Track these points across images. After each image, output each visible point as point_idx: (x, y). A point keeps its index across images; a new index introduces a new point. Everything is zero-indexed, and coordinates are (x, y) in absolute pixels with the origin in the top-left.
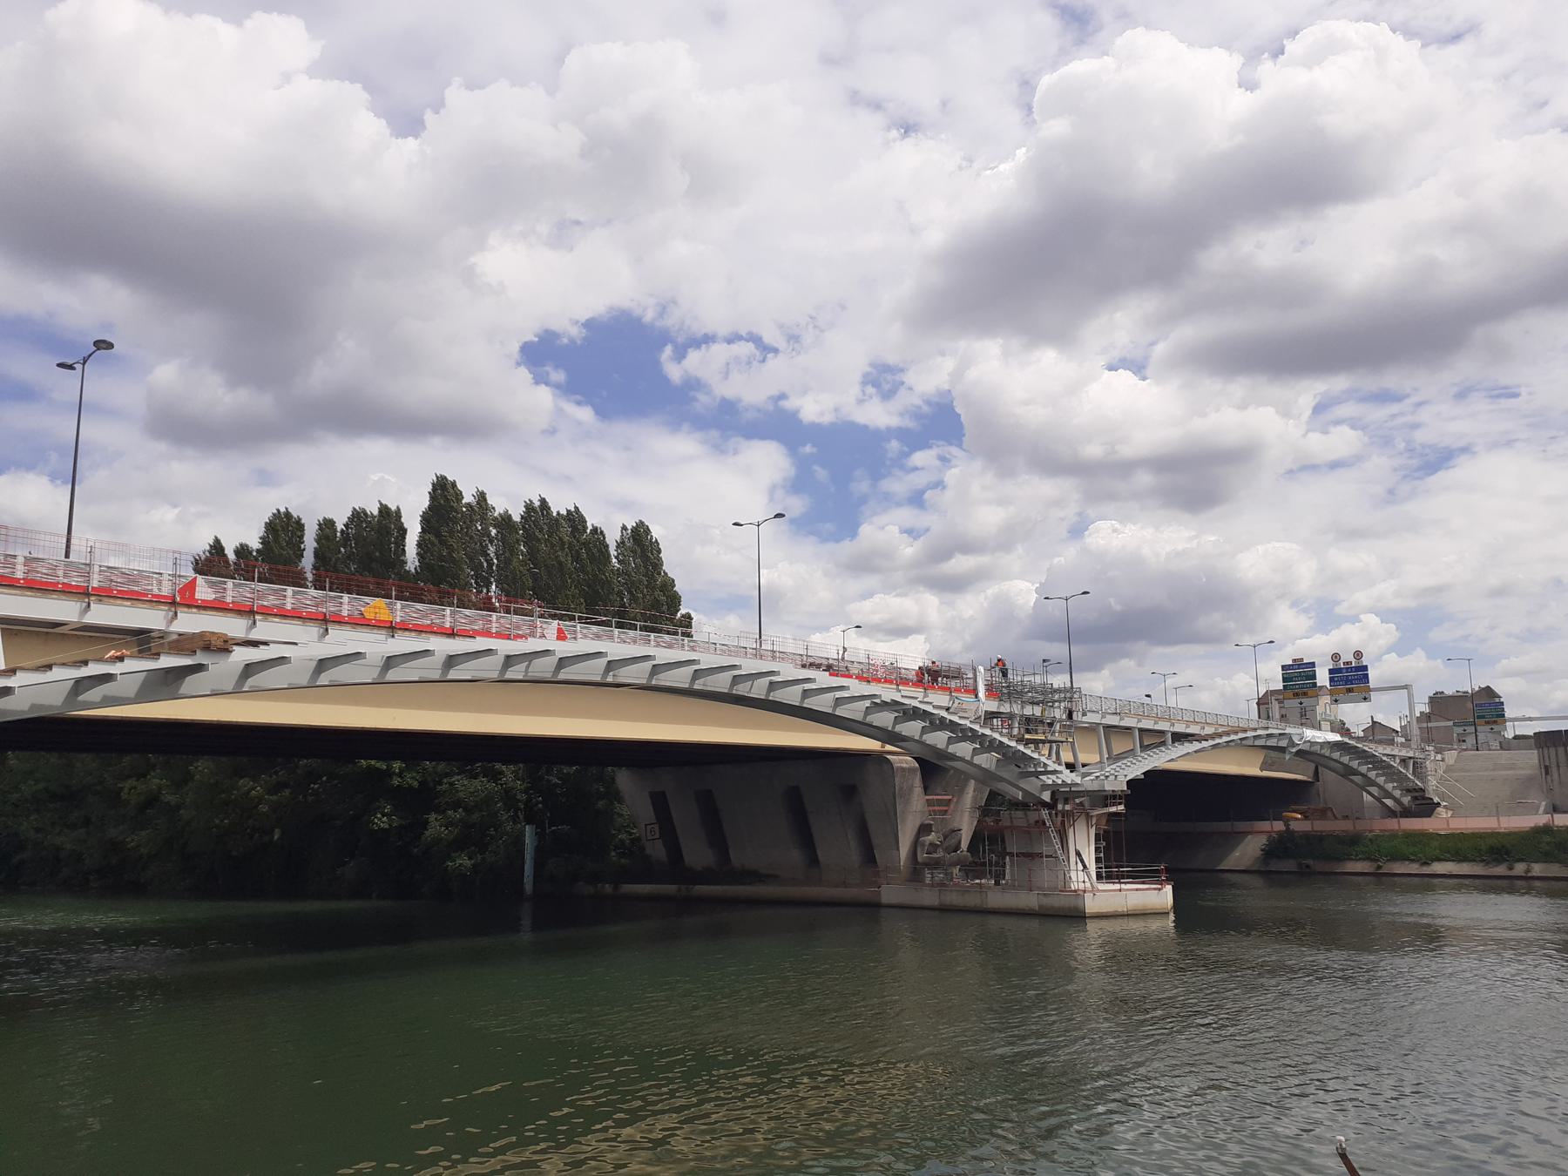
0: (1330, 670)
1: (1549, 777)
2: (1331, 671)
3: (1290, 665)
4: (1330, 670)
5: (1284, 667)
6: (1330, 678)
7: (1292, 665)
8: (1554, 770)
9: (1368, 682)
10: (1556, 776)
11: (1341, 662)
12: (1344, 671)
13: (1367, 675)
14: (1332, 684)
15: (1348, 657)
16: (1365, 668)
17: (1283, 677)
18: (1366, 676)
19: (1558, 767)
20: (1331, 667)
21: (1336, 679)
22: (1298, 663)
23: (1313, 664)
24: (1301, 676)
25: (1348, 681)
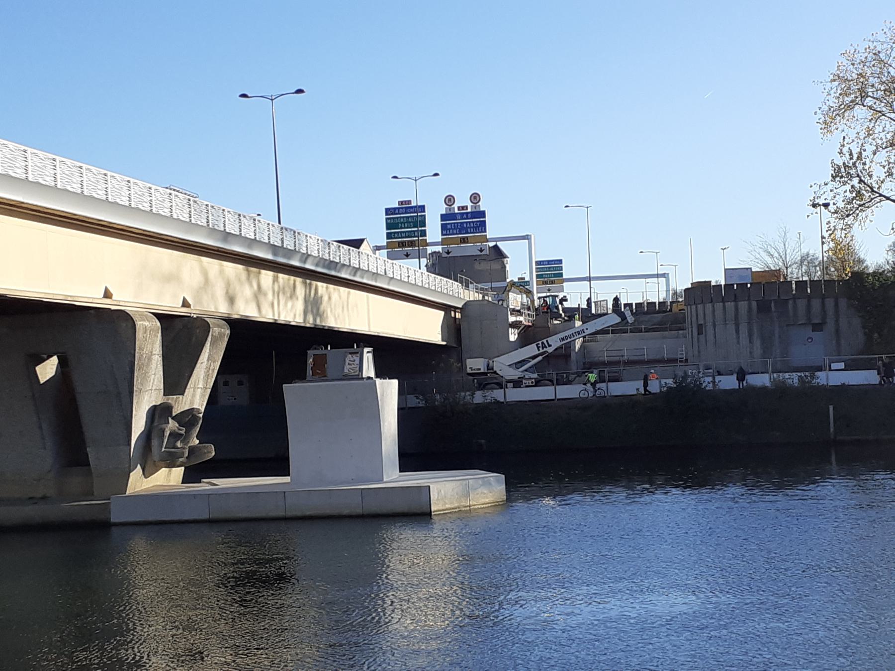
0: (442, 216)
1: (702, 337)
2: (443, 217)
3: (395, 209)
4: (442, 216)
5: (388, 211)
6: (442, 225)
7: (399, 209)
8: (710, 331)
9: (485, 231)
10: (711, 337)
11: (456, 206)
12: (459, 217)
13: (485, 222)
14: (445, 232)
15: (463, 200)
16: (482, 214)
17: (387, 224)
18: (483, 223)
19: (714, 326)
20: (444, 212)
21: (449, 226)
22: (405, 206)
23: (423, 208)
24: (408, 222)
25: (462, 229)
